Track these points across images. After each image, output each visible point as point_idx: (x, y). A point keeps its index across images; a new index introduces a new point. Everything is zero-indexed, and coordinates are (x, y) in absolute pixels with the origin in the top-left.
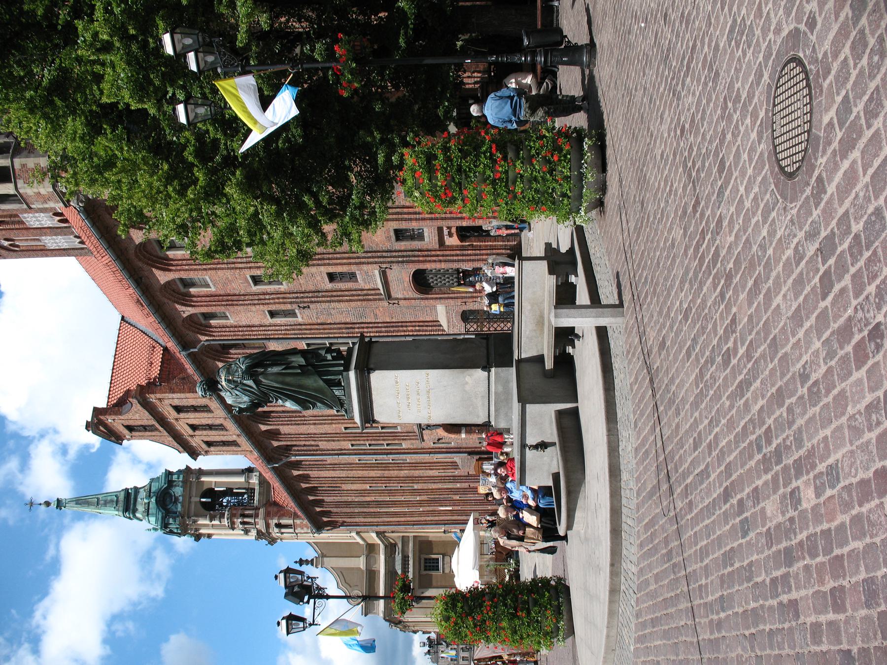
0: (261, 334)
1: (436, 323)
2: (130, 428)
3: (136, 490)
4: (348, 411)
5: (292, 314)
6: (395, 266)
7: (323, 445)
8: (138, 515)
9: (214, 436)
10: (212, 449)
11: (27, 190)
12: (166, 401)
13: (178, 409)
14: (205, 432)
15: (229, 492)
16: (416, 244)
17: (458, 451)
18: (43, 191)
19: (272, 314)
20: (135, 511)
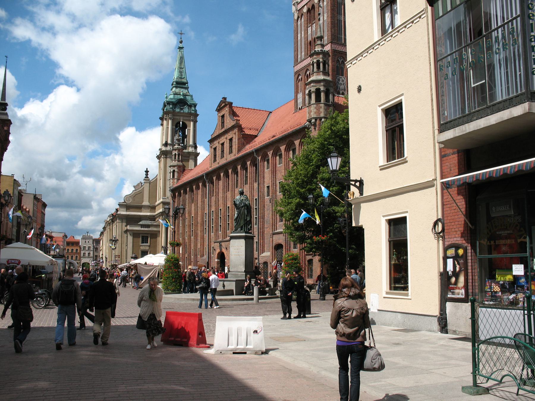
0: (261, 181)
1: (263, 251)
2: (223, 116)
3: (187, 88)
4: (234, 232)
5: (268, 195)
6: (284, 237)
7: (213, 198)
8: (174, 89)
9: (219, 152)
10: (213, 150)
11: (313, 108)
12: (234, 135)
13: (231, 140)
14: (220, 148)
15: (184, 136)
16: (292, 246)
17: (209, 257)
18: (312, 113)
19: (268, 187)
20: (176, 87)
